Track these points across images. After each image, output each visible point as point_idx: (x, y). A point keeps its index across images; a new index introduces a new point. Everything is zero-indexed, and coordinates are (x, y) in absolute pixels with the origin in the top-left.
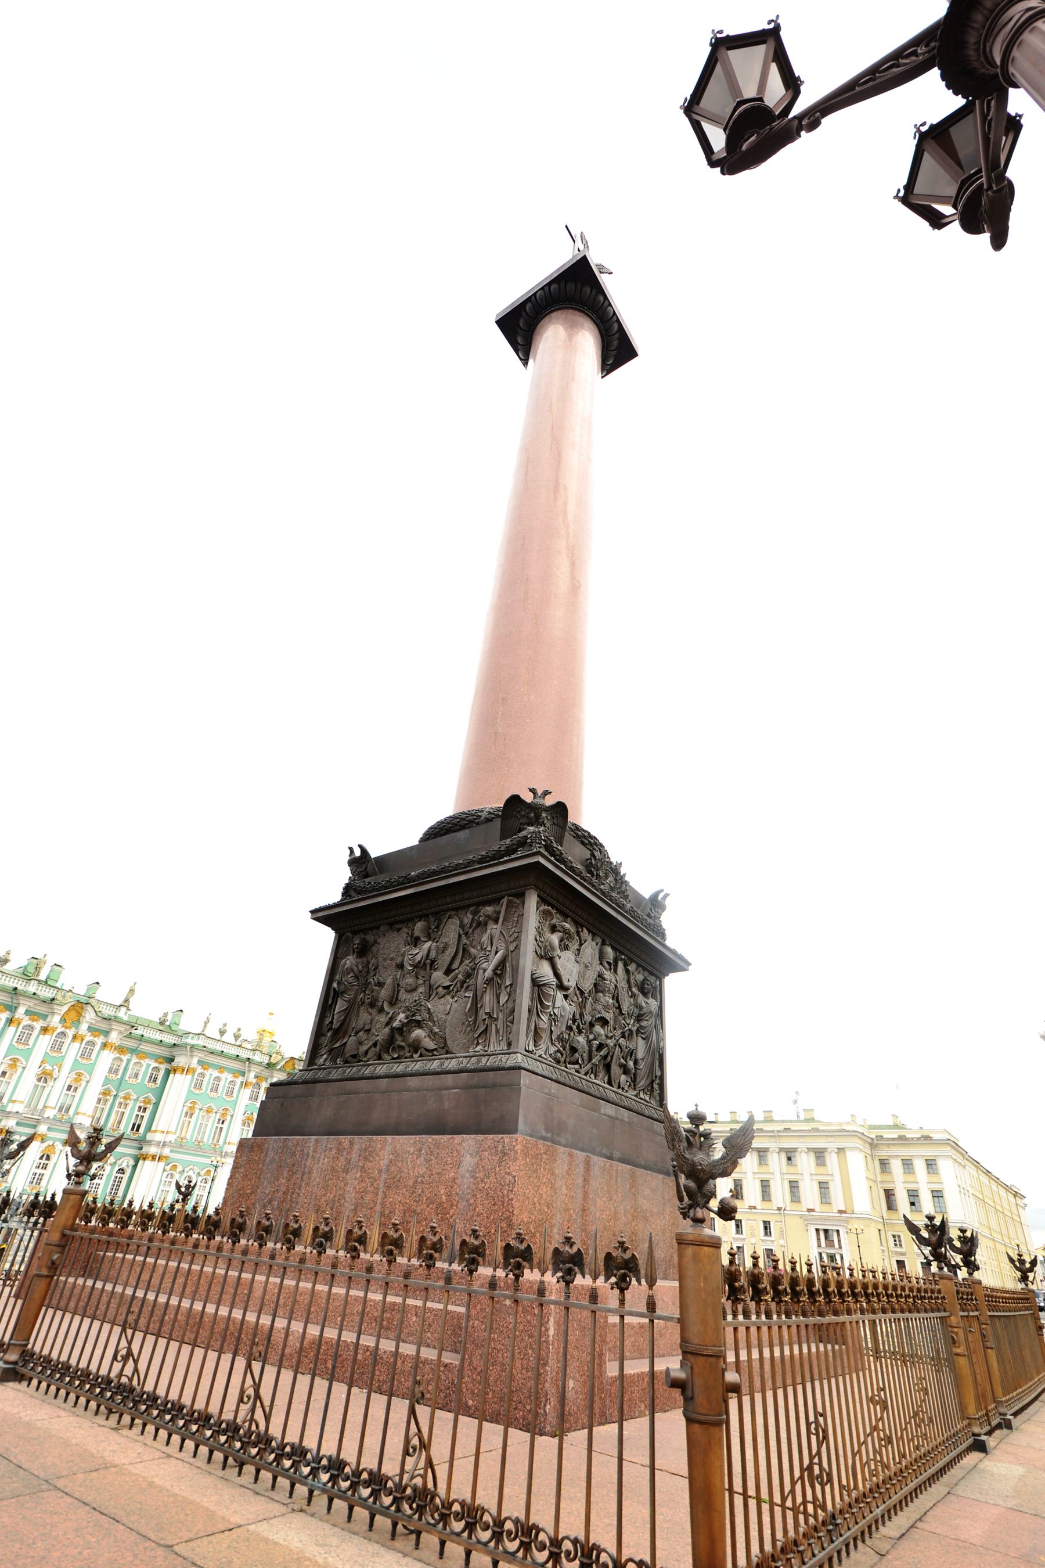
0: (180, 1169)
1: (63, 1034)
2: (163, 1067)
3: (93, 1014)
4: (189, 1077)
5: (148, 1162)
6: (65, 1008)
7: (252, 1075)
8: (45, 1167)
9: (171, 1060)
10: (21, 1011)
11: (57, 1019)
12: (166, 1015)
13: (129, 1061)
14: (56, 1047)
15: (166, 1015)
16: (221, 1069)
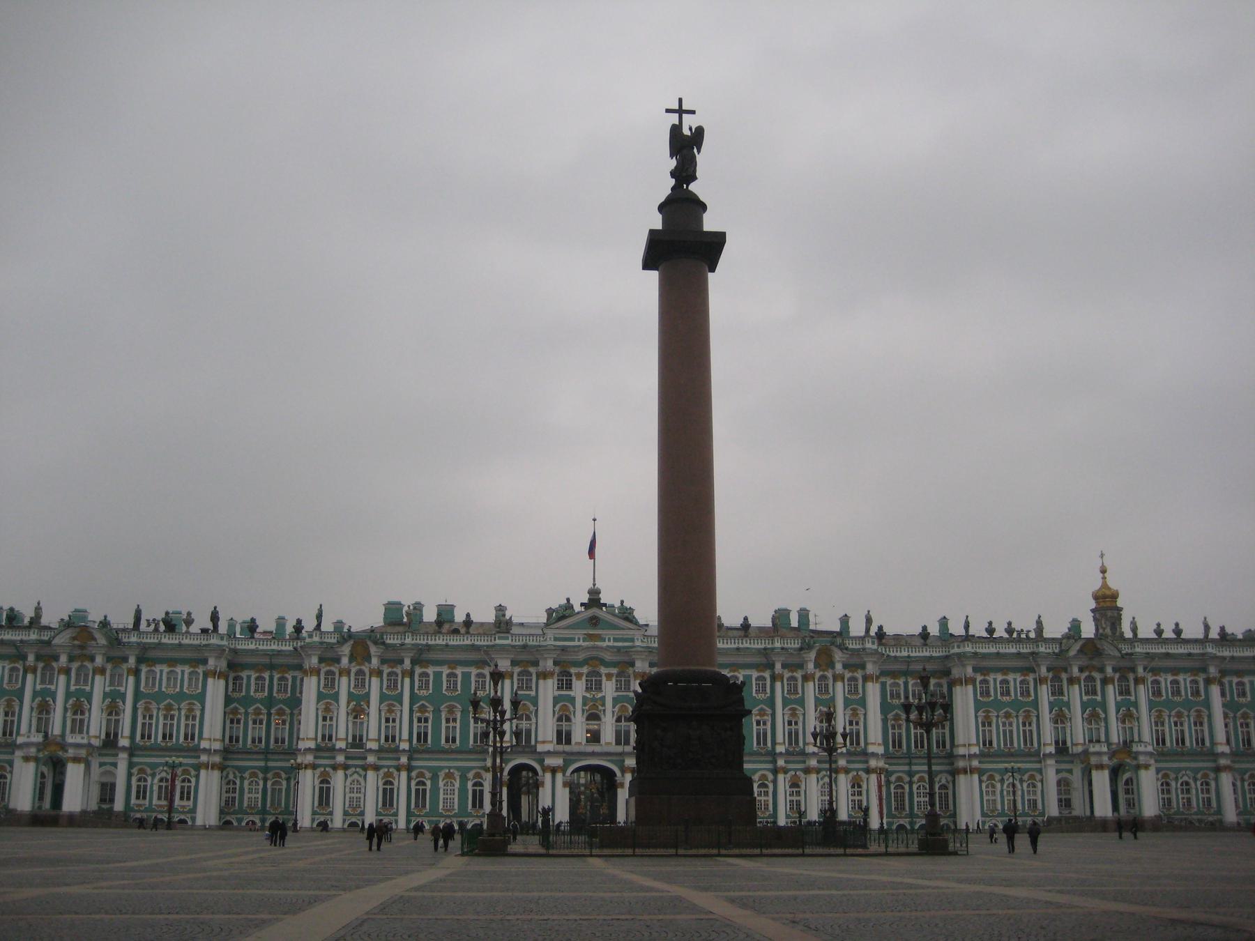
0: (998, 777)
1: (823, 678)
2: (944, 681)
3: (840, 654)
4: (970, 688)
5: (962, 779)
6: (813, 655)
7: (1043, 670)
8: (860, 794)
9: (947, 673)
10: (778, 666)
11: (811, 666)
12: (925, 628)
13: (906, 684)
14: (823, 689)
15: (925, 628)
16: (1005, 671)
